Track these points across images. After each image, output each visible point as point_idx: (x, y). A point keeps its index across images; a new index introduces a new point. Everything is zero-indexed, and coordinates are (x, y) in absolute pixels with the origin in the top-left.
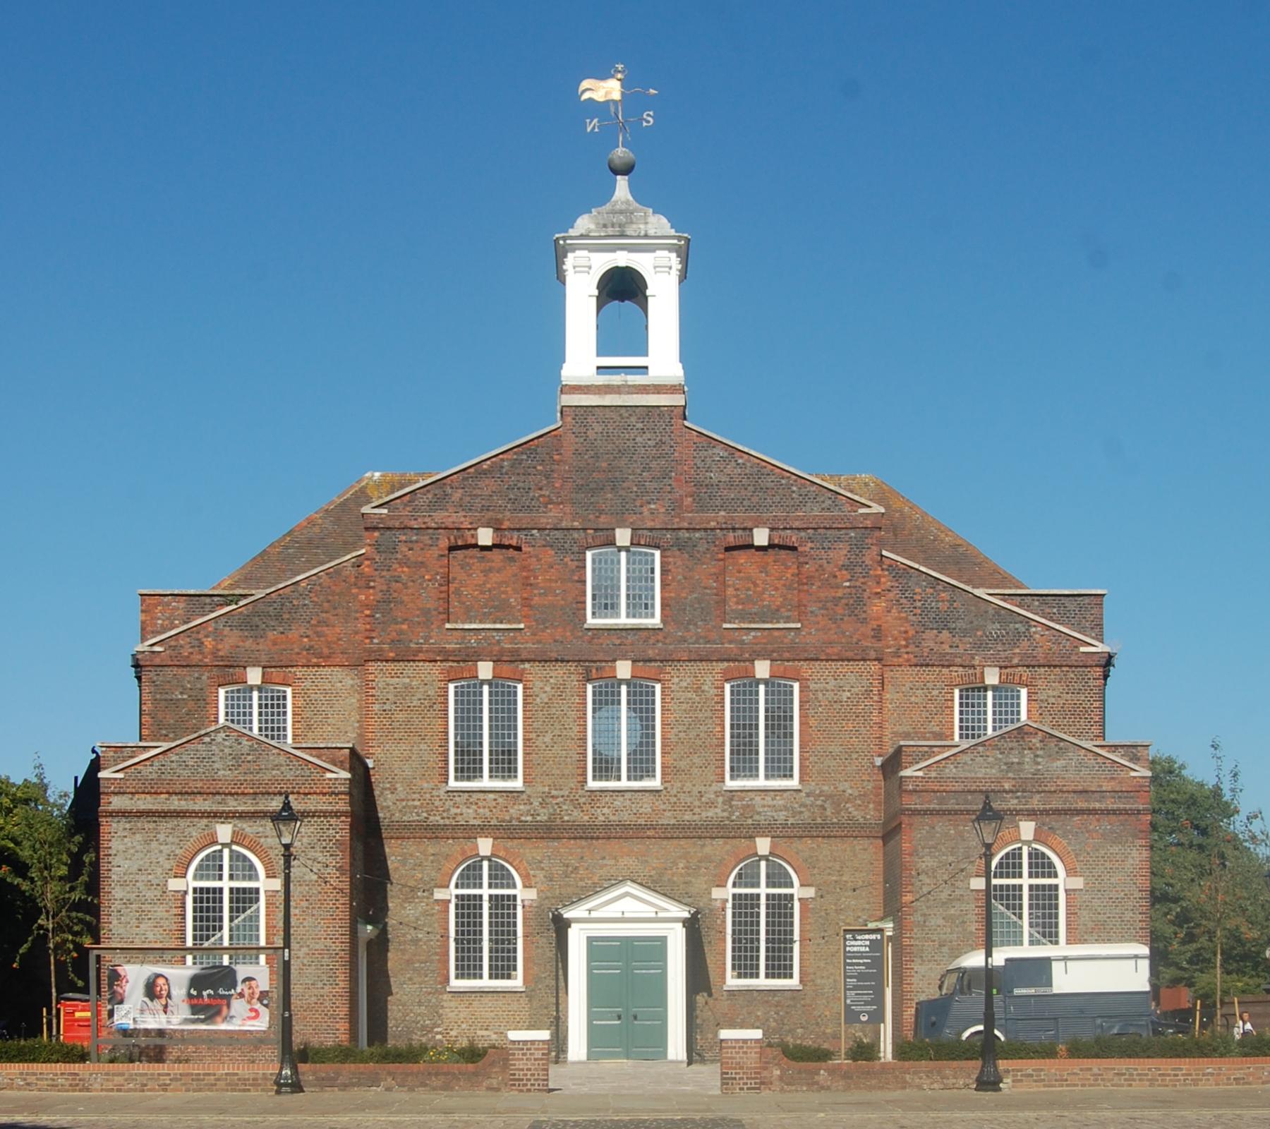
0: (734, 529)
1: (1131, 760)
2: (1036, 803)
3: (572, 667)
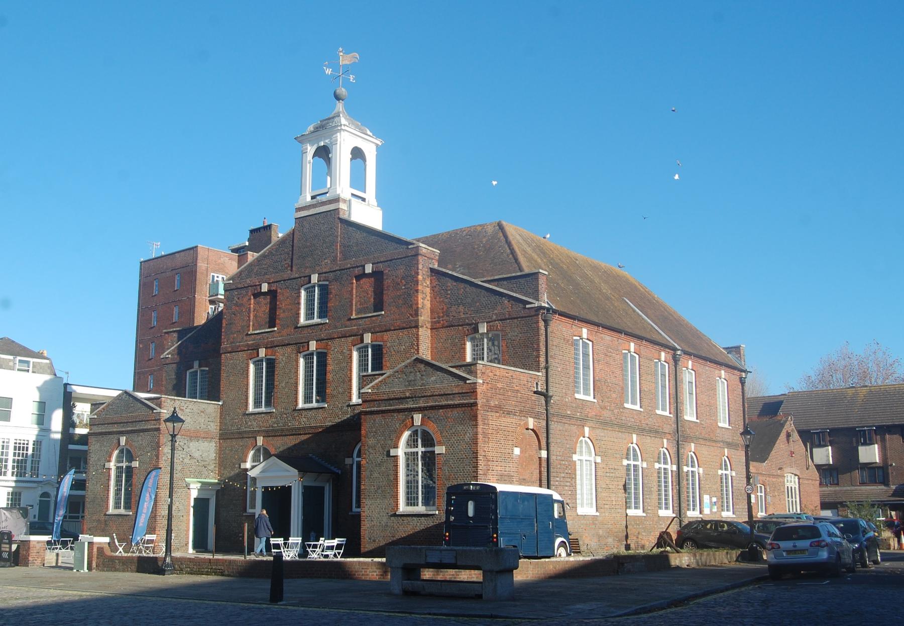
0: (358, 267)
1: (468, 373)
2: (422, 404)
3: (293, 347)
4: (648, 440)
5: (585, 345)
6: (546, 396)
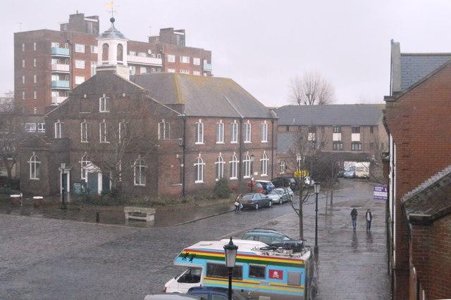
4: (227, 154)
5: (201, 124)
6: (184, 146)
